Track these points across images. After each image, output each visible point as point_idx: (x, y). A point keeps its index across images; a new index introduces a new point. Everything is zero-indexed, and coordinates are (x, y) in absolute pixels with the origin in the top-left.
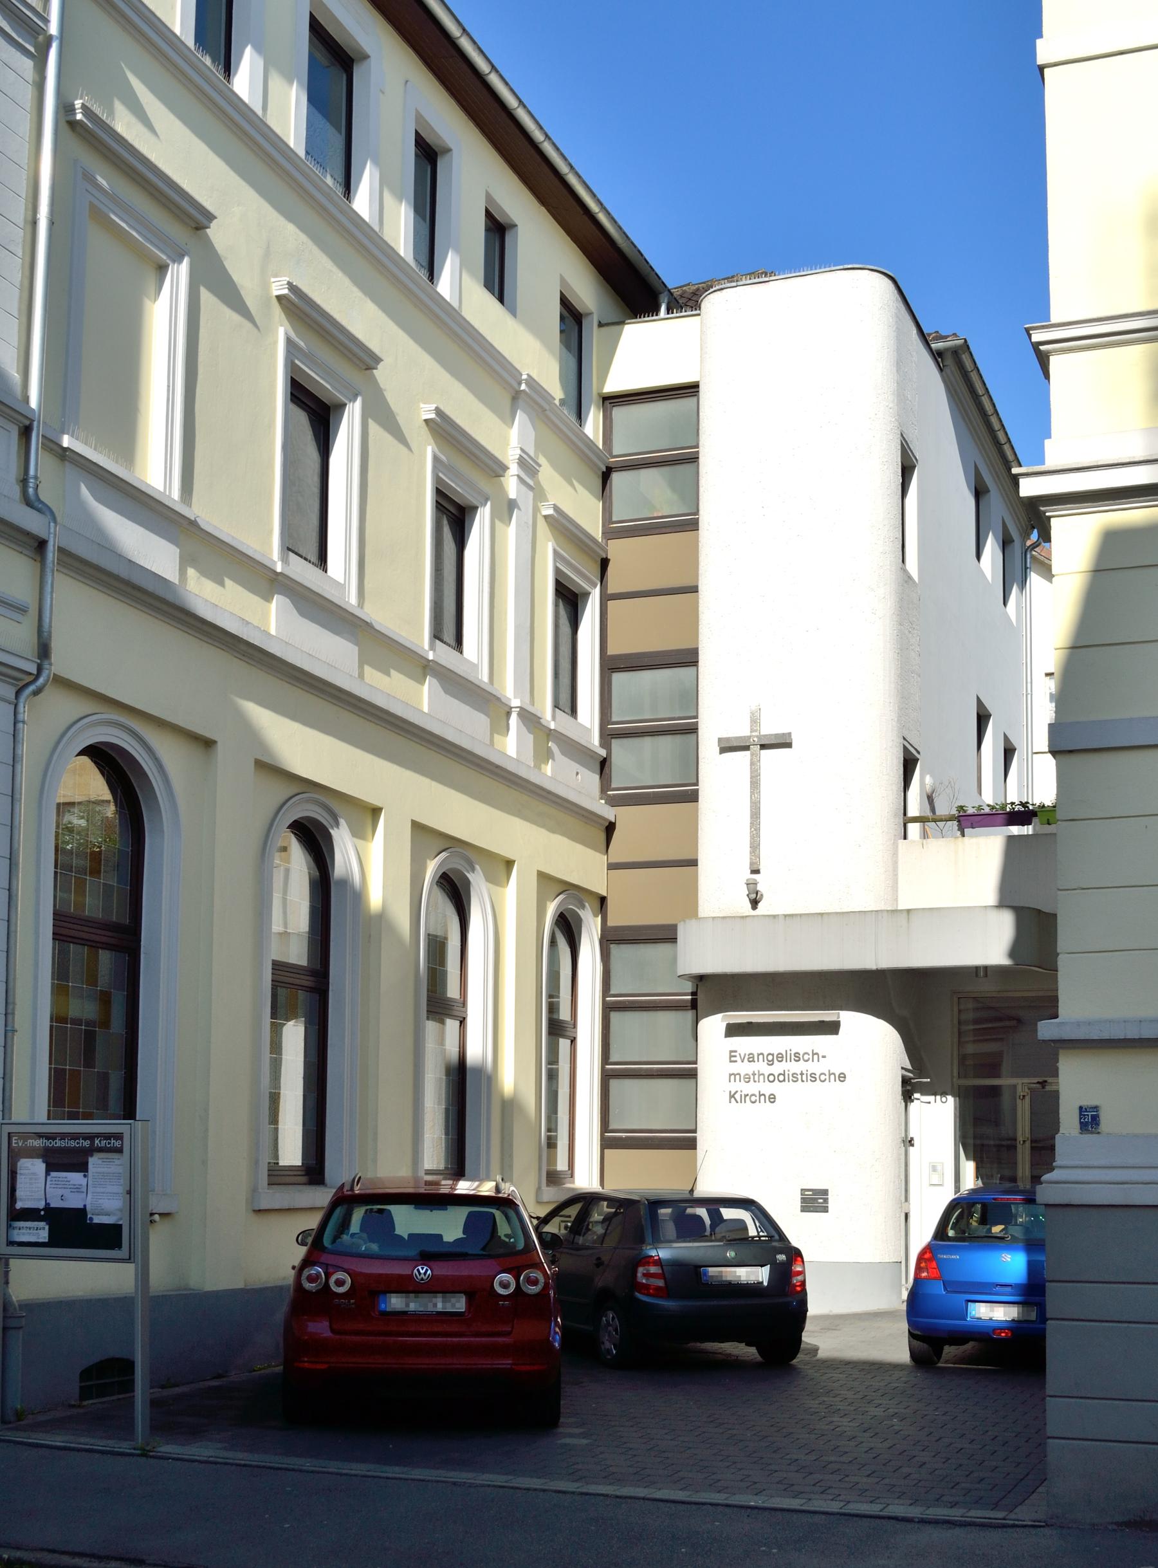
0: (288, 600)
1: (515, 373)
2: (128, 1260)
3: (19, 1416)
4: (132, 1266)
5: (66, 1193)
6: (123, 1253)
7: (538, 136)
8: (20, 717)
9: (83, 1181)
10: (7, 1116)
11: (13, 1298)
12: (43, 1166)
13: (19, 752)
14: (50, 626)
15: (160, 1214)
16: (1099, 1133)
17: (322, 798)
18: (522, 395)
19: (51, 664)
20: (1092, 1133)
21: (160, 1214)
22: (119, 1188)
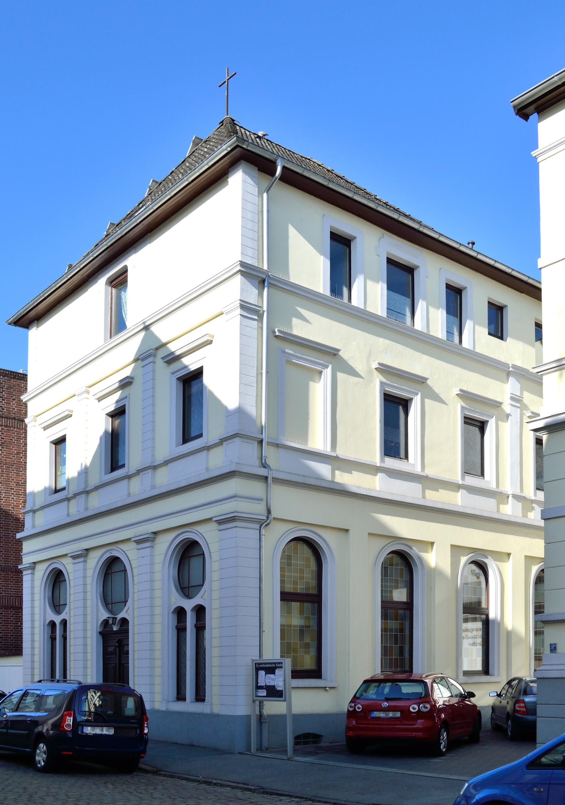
0: (385, 475)
1: (507, 365)
2: (285, 701)
3: (267, 749)
4: (286, 702)
5: (270, 680)
6: (283, 699)
7: (509, 271)
8: (262, 534)
9: (274, 677)
10: (261, 657)
11: (265, 713)
12: (265, 673)
13: (262, 544)
14: (270, 503)
15: (329, 687)
16: (556, 653)
17: (403, 542)
18: (511, 372)
19: (271, 515)
20: (554, 653)
21: (329, 687)
22: (282, 679)
